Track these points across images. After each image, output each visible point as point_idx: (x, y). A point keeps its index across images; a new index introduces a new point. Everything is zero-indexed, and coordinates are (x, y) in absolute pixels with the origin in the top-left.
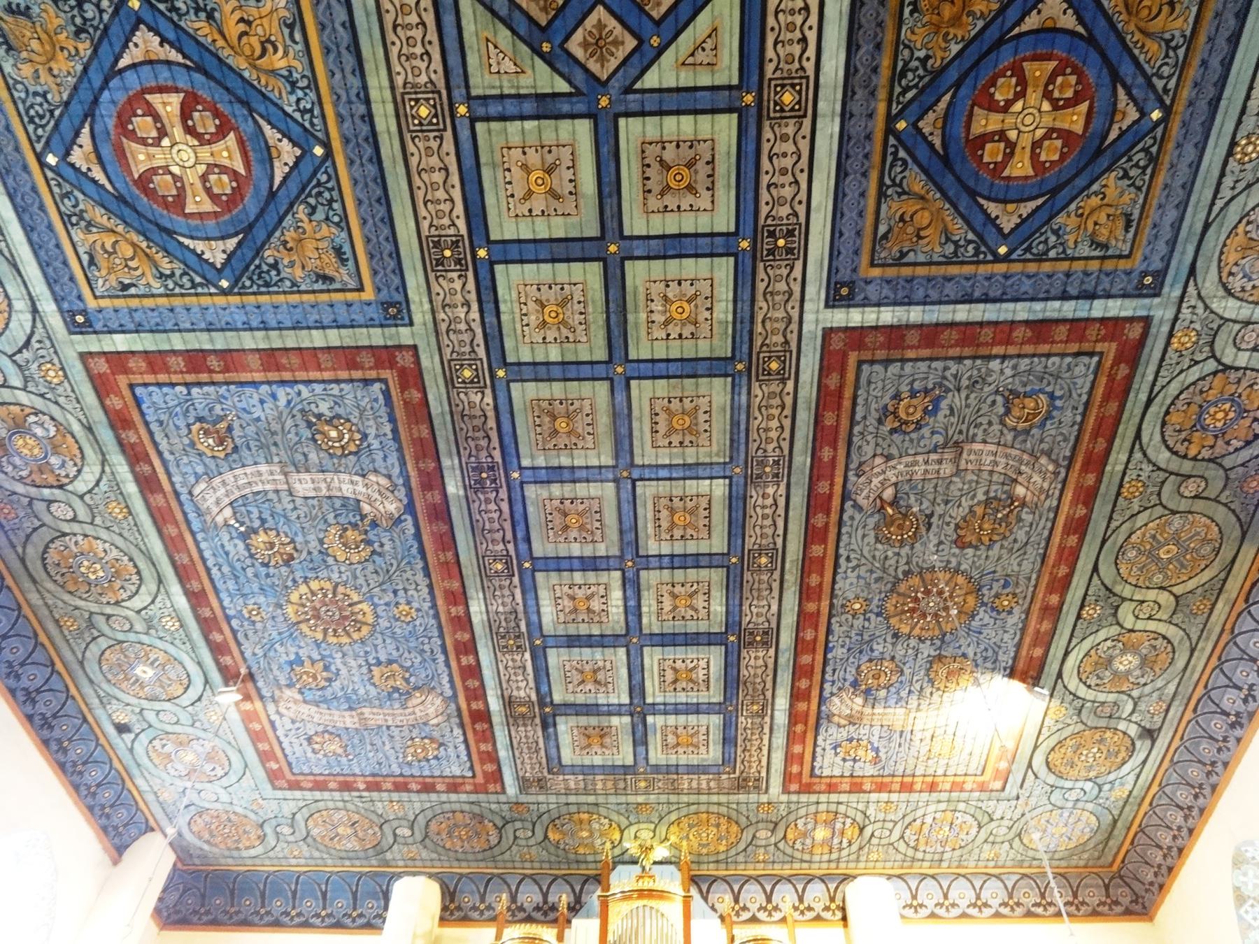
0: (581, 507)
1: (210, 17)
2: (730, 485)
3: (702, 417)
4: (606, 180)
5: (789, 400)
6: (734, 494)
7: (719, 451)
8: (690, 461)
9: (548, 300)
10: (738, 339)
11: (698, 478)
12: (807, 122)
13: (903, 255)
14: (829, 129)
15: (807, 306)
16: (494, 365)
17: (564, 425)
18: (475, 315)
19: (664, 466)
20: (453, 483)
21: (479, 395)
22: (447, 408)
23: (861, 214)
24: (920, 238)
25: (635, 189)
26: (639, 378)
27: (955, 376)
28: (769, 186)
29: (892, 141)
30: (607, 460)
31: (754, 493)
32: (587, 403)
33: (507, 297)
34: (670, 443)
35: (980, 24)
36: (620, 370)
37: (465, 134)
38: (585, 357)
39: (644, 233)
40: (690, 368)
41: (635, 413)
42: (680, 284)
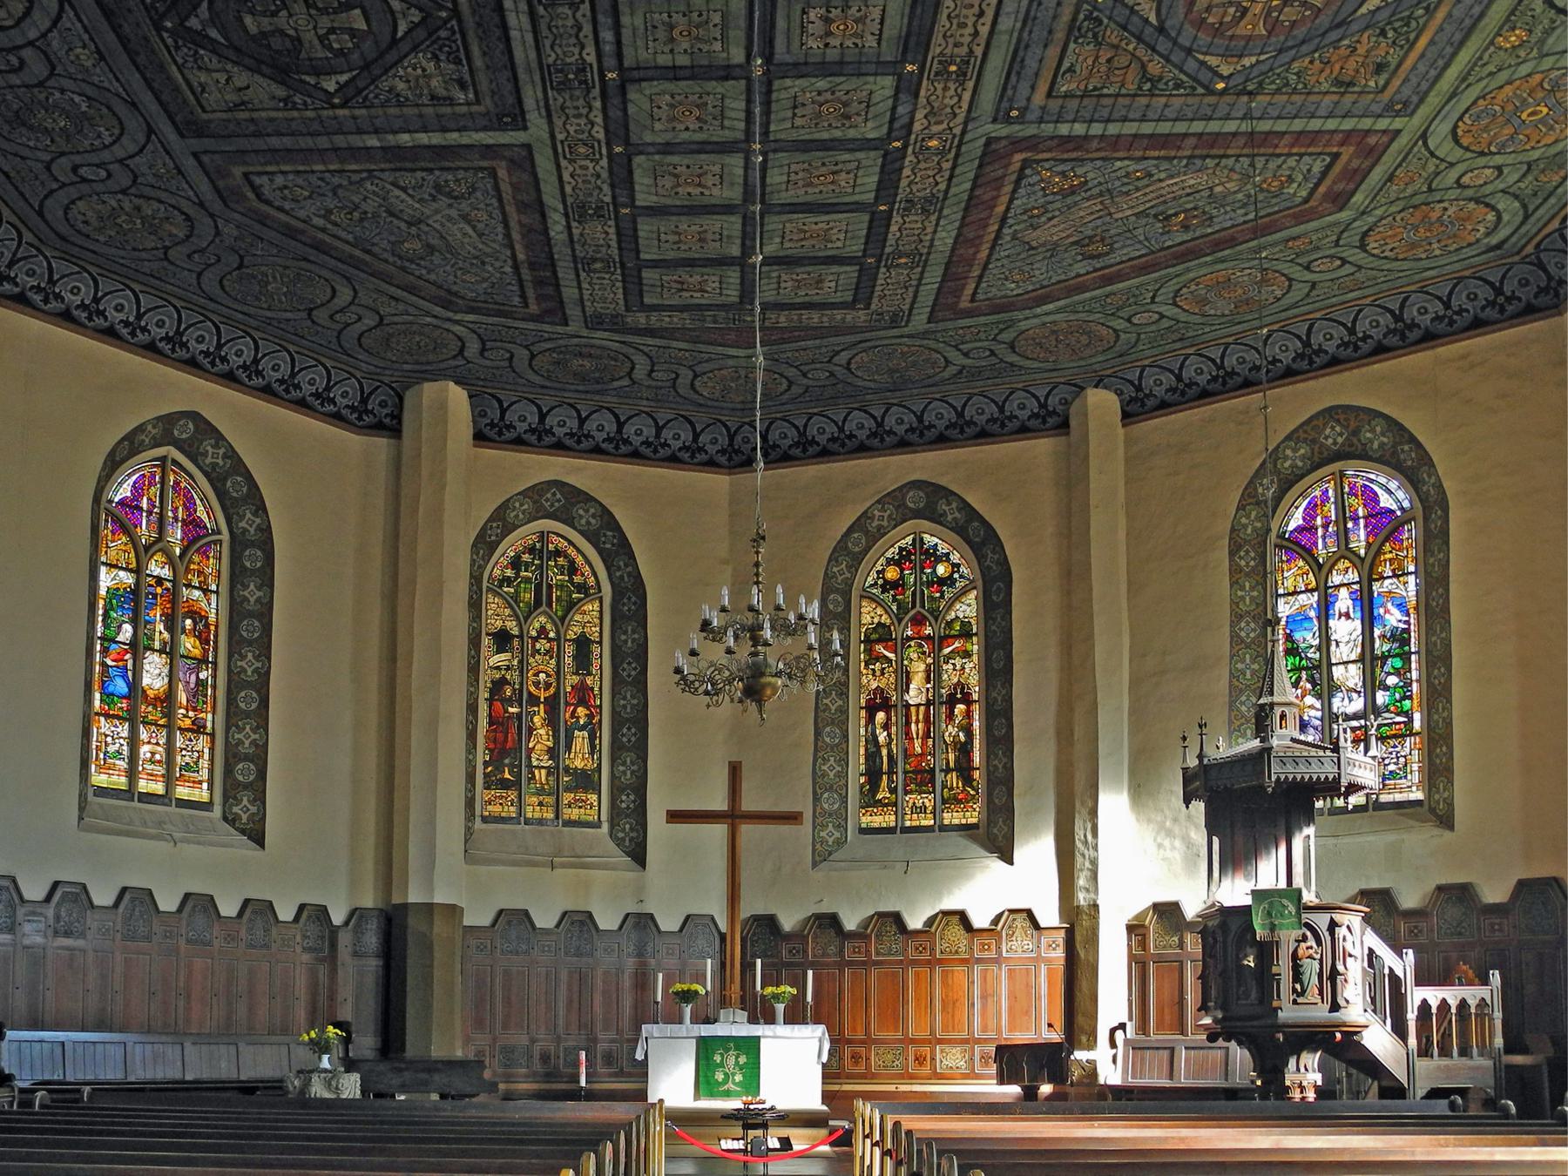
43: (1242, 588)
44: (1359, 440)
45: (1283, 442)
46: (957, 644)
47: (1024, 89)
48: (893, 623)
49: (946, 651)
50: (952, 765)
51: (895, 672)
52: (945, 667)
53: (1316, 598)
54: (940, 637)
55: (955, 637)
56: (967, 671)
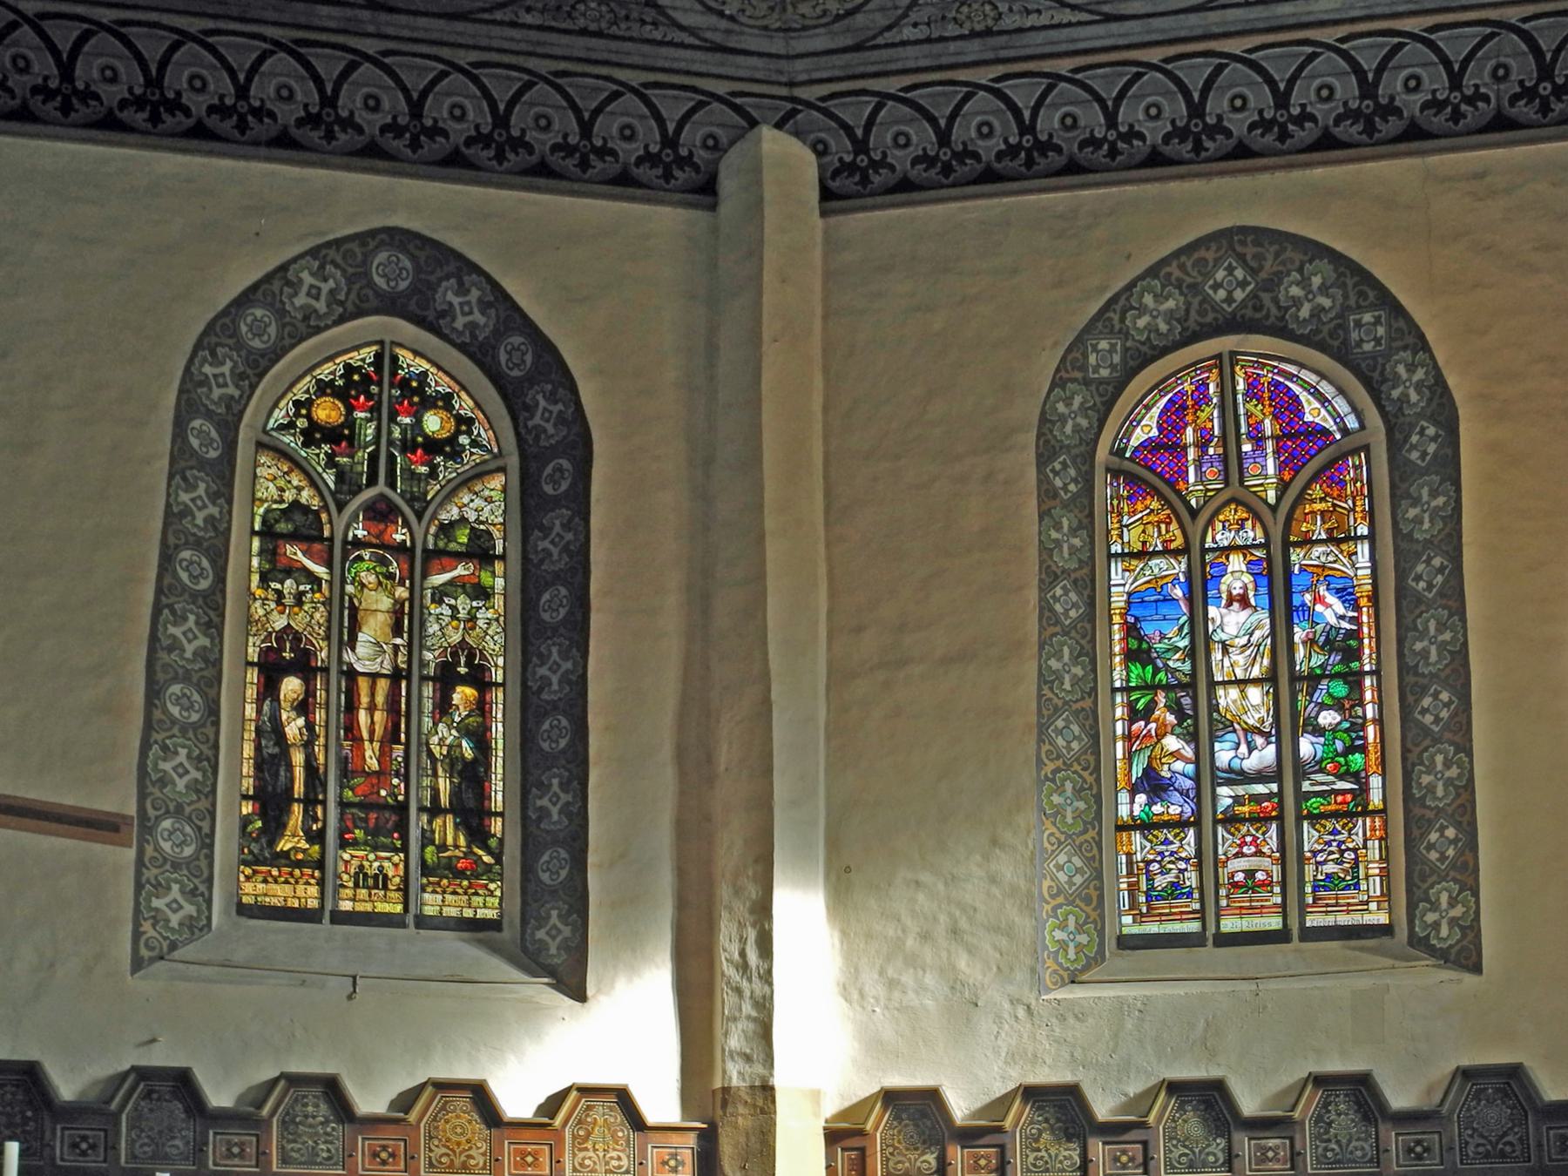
43: (1058, 527)
44: (1276, 301)
45: (1141, 277)
46: (460, 570)
48: (326, 507)
49: (439, 579)
50: (444, 800)
51: (328, 603)
52: (434, 609)
53: (1183, 566)
54: (425, 551)
55: (459, 556)
56: (480, 623)
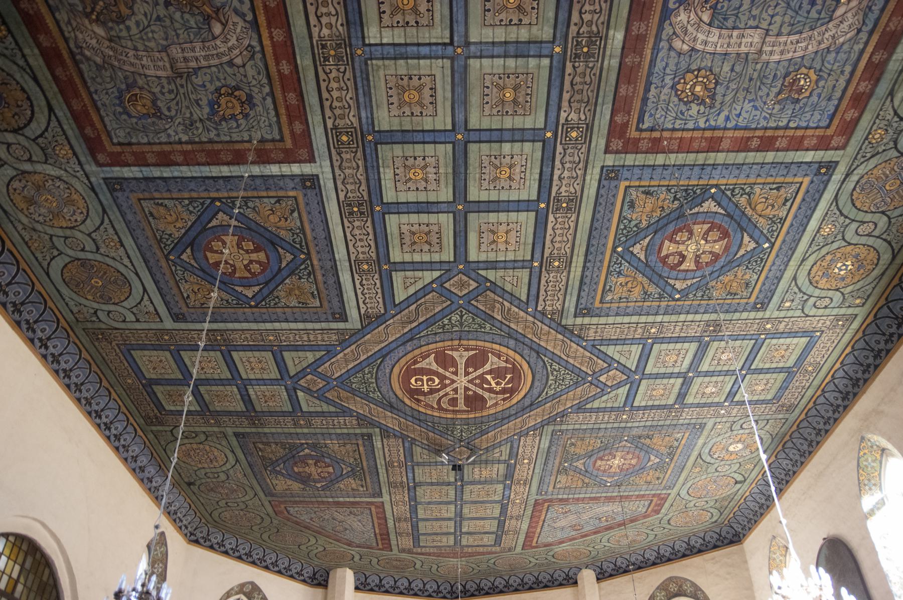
0: (503, 16)
1: (645, 293)
2: (363, 38)
3: (394, 99)
4: (463, 238)
5: (328, 113)
6: (359, 28)
7: (378, 70)
8: (402, 62)
9: (506, 180)
10: (374, 156)
11: (394, 45)
12: (353, 258)
13: (278, 201)
14: (340, 253)
15: (331, 176)
16: (553, 140)
17: (508, 95)
18: (557, 173)
19: (424, 58)
20: (616, 42)
21: (569, 119)
22: (598, 109)
23: (311, 222)
24: (271, 210)
25: (446, 233)
26: (445, 131)
27: (208, 130)
28: (368, 234)
29: (305, 251)
30: (474, 63)
31: (340, 28)
32: (487, 112)
33: (532, 182)
34: (420, 79)
35: (279, 288)
36: (459, 137)
37: (537, 255)
38: (484, 146)
39: (440, 215)
40: (405, 137)
41: (448, 104)
42: (417, 189)
47: (545, 487)
